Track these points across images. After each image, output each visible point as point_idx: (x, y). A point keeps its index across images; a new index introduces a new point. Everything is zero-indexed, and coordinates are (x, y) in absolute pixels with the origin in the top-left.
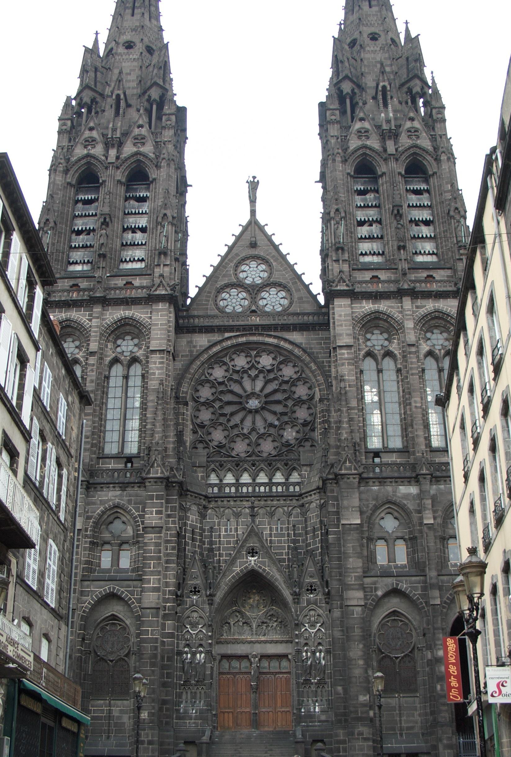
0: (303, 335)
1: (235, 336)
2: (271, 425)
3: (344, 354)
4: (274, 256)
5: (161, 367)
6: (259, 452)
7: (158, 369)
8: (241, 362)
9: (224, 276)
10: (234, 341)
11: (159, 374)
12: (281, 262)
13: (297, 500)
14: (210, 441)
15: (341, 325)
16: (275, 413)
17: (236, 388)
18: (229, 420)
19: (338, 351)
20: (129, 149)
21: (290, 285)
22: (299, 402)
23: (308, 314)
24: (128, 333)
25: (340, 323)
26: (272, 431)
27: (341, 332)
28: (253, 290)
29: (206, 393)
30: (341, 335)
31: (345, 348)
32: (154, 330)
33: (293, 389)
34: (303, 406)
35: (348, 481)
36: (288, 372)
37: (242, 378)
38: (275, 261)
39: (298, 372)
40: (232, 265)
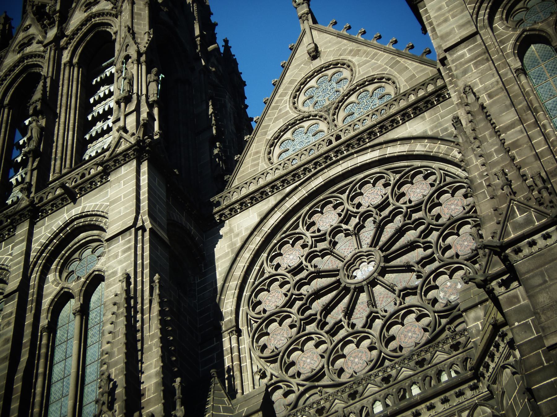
0: (424, 119)
1: (300, 185)
2: (408, 292)
3: (463, 56)
4: (351, 51)
5: (125, 258)
6: (395, 350)
7: (121, 262)
8: (327, 220)
9: (277, 119)
10: (303, 192)
11: (122, 269)
12: (365, 52)
13: (474, 388)
14: (293, 377)
15: (446, 20)
16: (408, 268)
17: (327, 263)
18: (322, 325)
19: (449, 58)
20: (77, 18)
21: (389, 71)
22: (455, 225)
23: (424, 85)
24: (85, 245)
25: (442, 19)
26: (410, 300)
27: (448, 29)
28: (328, 111)
29: (273, 299)
30: (448, 34)
31: (462, 45)
32: (113, 210)
33: (435, 211)
34: (461, 231)
35: (535, 249)
36: (417, 191)
37: (335, 243)
38: (354, 55)
39: (435, 181)
40: (287, 98)
